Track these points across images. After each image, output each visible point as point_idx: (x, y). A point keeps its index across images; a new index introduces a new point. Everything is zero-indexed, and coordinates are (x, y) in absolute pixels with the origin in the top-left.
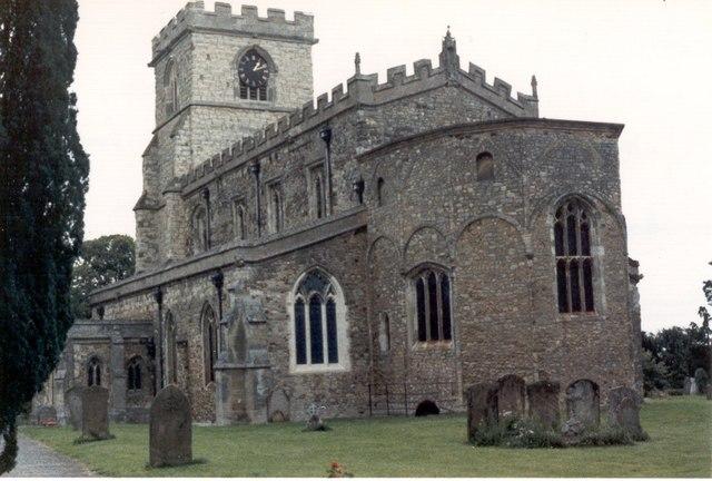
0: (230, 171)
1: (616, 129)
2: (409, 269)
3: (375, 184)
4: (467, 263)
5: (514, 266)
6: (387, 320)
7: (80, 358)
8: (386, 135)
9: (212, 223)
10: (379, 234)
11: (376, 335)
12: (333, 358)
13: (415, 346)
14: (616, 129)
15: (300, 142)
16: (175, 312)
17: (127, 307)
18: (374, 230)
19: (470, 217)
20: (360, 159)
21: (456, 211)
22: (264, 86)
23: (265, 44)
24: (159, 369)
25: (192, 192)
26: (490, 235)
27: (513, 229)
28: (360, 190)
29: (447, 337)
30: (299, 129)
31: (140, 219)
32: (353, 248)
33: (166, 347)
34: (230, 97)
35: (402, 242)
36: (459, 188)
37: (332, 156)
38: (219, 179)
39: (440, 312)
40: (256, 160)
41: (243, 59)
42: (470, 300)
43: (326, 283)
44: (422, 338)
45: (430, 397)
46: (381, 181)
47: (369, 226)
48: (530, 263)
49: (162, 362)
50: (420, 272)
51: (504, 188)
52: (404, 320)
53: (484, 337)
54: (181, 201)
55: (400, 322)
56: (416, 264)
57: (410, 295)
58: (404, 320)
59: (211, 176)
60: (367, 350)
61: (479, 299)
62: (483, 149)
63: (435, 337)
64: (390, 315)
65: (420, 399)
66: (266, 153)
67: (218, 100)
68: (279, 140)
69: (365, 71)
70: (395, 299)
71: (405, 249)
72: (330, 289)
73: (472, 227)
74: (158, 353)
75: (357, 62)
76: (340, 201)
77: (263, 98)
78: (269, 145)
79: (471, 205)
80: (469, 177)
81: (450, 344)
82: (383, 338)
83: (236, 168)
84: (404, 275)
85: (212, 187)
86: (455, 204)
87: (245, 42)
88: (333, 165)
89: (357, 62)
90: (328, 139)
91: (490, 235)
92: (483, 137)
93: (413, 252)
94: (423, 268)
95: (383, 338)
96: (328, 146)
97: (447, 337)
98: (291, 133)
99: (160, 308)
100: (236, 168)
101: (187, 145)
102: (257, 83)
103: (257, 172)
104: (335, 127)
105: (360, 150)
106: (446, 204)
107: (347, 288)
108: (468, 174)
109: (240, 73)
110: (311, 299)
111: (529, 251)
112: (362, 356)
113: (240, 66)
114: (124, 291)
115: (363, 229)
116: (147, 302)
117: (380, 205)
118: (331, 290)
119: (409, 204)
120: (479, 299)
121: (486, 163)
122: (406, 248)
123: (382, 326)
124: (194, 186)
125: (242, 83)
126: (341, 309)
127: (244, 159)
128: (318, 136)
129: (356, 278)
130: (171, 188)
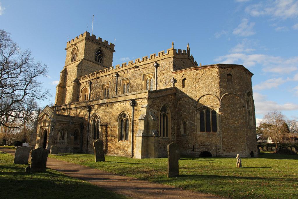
1: (253, 75)
2: (198, 108)
4: (224, 107)
6: (185, 123)
7: (58, 128)
11: (179, 128)
13: (199, 133)
14: (253, 75)
15: (141, 67)
22: (102, 59)
23: (102, 48)
26: (231, 99)
27: (239, 98)
34: (93, 59)
41: (97, 51)
44: (202, 130)
45: (207, 150)
46: (184, 80)
49: (88, 131)
50: (204, 109)
52: (196, 124)
57: (198, 116)
60: (175, 134)
61: (228, 119)
64: (187, 123)
65: (202, 150)
77: (100, 63)
80: (225, 80)
82: (182, 130)
84: (197, 110)
91: (231, 99)
95: (182, 130)
97: (215, 130)
101: (80, 70)
102: (100, 58)
109: (96, 54)
113: (96, 53)
120: (228, 119)
121: (229, 77)
123: (182, 126)
126: (170, 119)
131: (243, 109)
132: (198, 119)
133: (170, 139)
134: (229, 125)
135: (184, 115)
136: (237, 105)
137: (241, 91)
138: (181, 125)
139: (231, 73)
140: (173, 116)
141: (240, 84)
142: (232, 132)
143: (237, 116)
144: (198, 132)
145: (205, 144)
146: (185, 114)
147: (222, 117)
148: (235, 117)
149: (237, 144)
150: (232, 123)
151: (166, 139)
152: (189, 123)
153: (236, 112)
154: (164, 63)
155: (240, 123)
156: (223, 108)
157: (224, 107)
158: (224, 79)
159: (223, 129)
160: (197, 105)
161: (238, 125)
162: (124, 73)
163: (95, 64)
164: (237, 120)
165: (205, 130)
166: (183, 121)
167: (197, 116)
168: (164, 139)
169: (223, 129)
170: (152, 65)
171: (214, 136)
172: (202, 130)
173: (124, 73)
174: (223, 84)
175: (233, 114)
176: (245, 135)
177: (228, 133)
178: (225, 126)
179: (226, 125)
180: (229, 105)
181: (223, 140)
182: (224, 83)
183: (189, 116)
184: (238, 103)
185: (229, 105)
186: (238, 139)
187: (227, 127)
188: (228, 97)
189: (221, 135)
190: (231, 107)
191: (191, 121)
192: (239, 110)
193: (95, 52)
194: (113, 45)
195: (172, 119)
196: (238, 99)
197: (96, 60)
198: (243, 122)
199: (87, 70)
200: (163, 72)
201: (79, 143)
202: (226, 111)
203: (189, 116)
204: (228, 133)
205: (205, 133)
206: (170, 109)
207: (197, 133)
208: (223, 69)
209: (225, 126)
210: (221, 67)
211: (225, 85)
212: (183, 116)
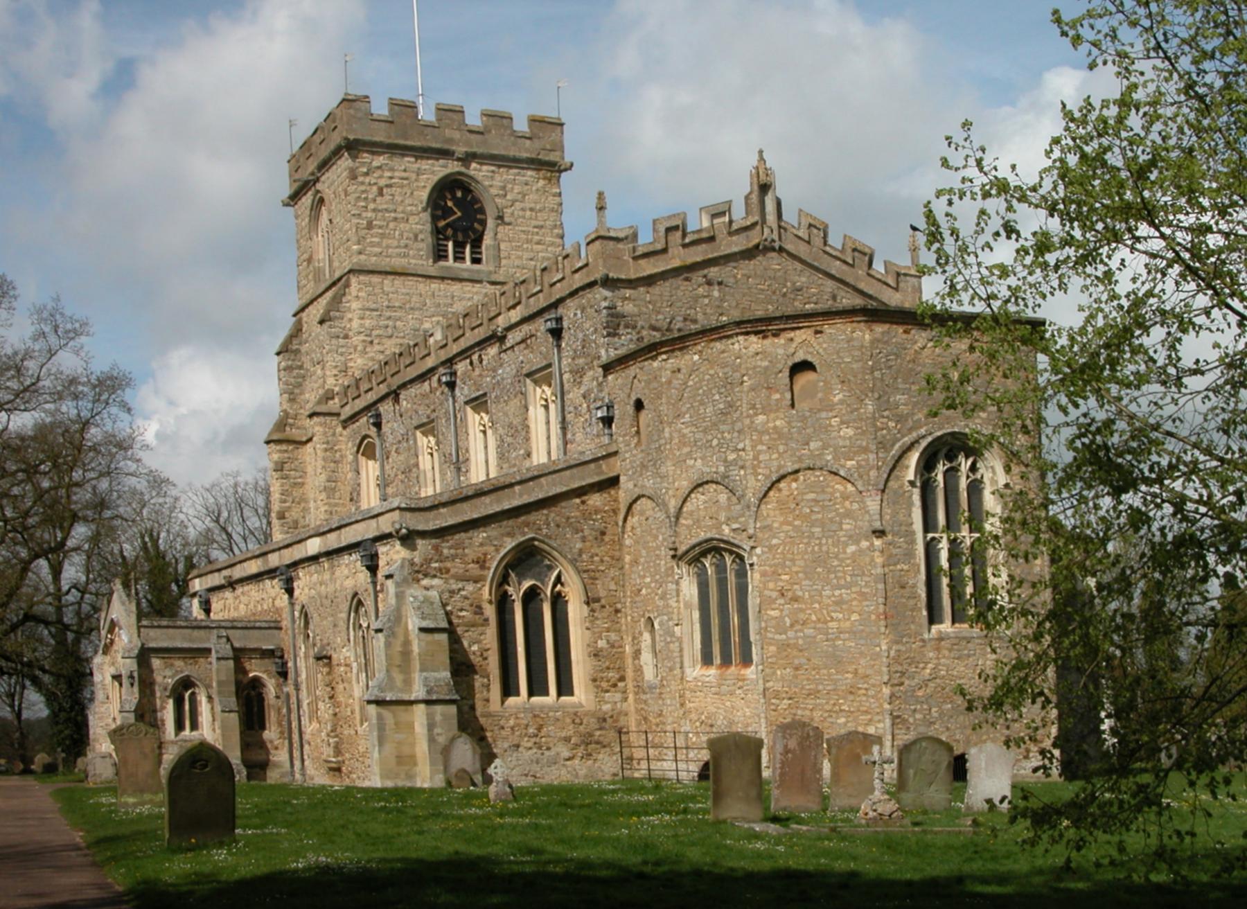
0: (412, 381)
2: (682, 549)
3: (630, 409)
4: (775, 541)
5: (851, 549)
8: (654, 328)
9: (387, 467)
10: (638, 491)
12: (565, 687)
13: (695, 671)
16: (311, 610)
17: (244, 599)
18: (630, 485)
19: (780, 467)
20: (608, 368)
21: (756, 458)
24: (293, 700)
25: (354, 418)
26: (812, 496)
27: (850, 487)
28: (608, 421)
29: (747, 660)
30: (515, 316)
31: (276, 457)
32: (596, 512)
33: (301, 664)
35: (673, 504)
36: (761, 418)
37: (564, 362)
38: (394, 395)
39: (735, 620)
40: (450, 362)
42: (782, 601)
43: (550, 568)
46: (639, 405)
47: (622, 479)
48: (878, 543)
49: (297, 688)
50: (704, 554)
51: (835, 421)
53: (804, 661)
54: (339, 429)
55: (672, 635)
56: (694, 541)
57: (690, 589)
58: (677, 629)
59: (383, 389)
61: (795, 599)
62: (799, 357)
63: (726, 661)
64: (656, 626)
66: (465, 353)
67: (398, 263)
68: (481, 333)
69: (616, 222)
70: (663, 597)
71: (677, 518)
72: (558, 580)
73: (782, 485)
74: (291, 675)
75: (601, 208)
76: (579, 436)
78: (470, 338)
79: (781, 448)
81: (750, 672)
83: (423, 377)
85: (386, 408)
86: (753, 447)
87: (439, 170)
88: (566, 376)
89: (601, 208)
90: (557, 333)
91: (812, 496)
92: (799, 336)
93: (690, 522)
94: (713, 548)
95: (646, 658)
96: (559, 346)
97: (747, 660)
98: (502, 322)
99: (292, 604)
100: (423, 377)
103: (451, 385)
104: (569, 312)
105: (606, 355)
106: (741, 446)
107: (589, 578)
108: (777, 396)
110: (525, 594)
111: (877, 525)
112: (615, 685)
114: (238, 572)
115: (614, 482)
116: (273, 592)
117: (639, 443)
118: (558, 580)
119: (683, 443)
120: (795, 599)
121: (804, 379)
122: (678, 516)
123: (647, 636)
124: (360, 404)
125: (438, 232)
126: (576, 611)
127: (430, 362)
128: (541, 326)
129: (602, 561)
130: (323, 409)
131: (872, 544)
132: (688, 605)
133: (581, 705)
134: (801, 631)
135: (648, 586)
136: (841, 523)
137: (866, 450)
138: (641, 634)
139: (810, 359)
140: (602, 593)
141: (857, 410)
142: (815, 661)
143: (842, 582)
144: (688, 671)
145: (712, 726)
146: (648, 580)
147: (767, 593)
148: (834, 588)
149: (842, 720)
150: (814, 618)
151: (551, 708)
152: (661, 624)
153: (836, 563)
154: (579, 312)
155: (855, 617)
156: (771, 547)
157: (775, 541)
158: (777, 396)
159: (773, 648)
160: (676, 534)
161: (848, 624)
162: (471, 363)
163: (435, 285)
164: (839, 602)
165: (717, 660)
166: (647, 615)
167: (678, 592)
168: (532, 709)
169: (773, 648)
170: (541, 326)
171: (740, 683)
172: (707, 659)
173: (471, 363)
174: (768, 421)
175: (819, 574)
176: (880, 673)
177: (797, 669)
178: (777, 637)
179: (785, 633)
180: (796, 528)
181: (768, 703)
182: (772, 416)
183: (659, 592)
184: (848, 514)
185: (796, 528)
186: (844, 698)
187: (788, 638)
188: (794, 485)
189: (761, 682)
190: (812, 534)
191: (665, 618)
192: (851, 549)
193: (425, 210)
194: (546, 126)
195: (593, 611)
196: (845, 497)
197: (439, 255)
198: (871, 612)
199: (390, 331)
200: (581, 361)
201: (276, 743)
202: (785, 559)
203: (659, 592)
204: (797, 669)
205: (712, 671)
206: (573, 562)
207: (683, 673)
208: (768, 342)
209: (777, 637)
210: (756, 333)
211: (778, 423)
212: (644, 591)
